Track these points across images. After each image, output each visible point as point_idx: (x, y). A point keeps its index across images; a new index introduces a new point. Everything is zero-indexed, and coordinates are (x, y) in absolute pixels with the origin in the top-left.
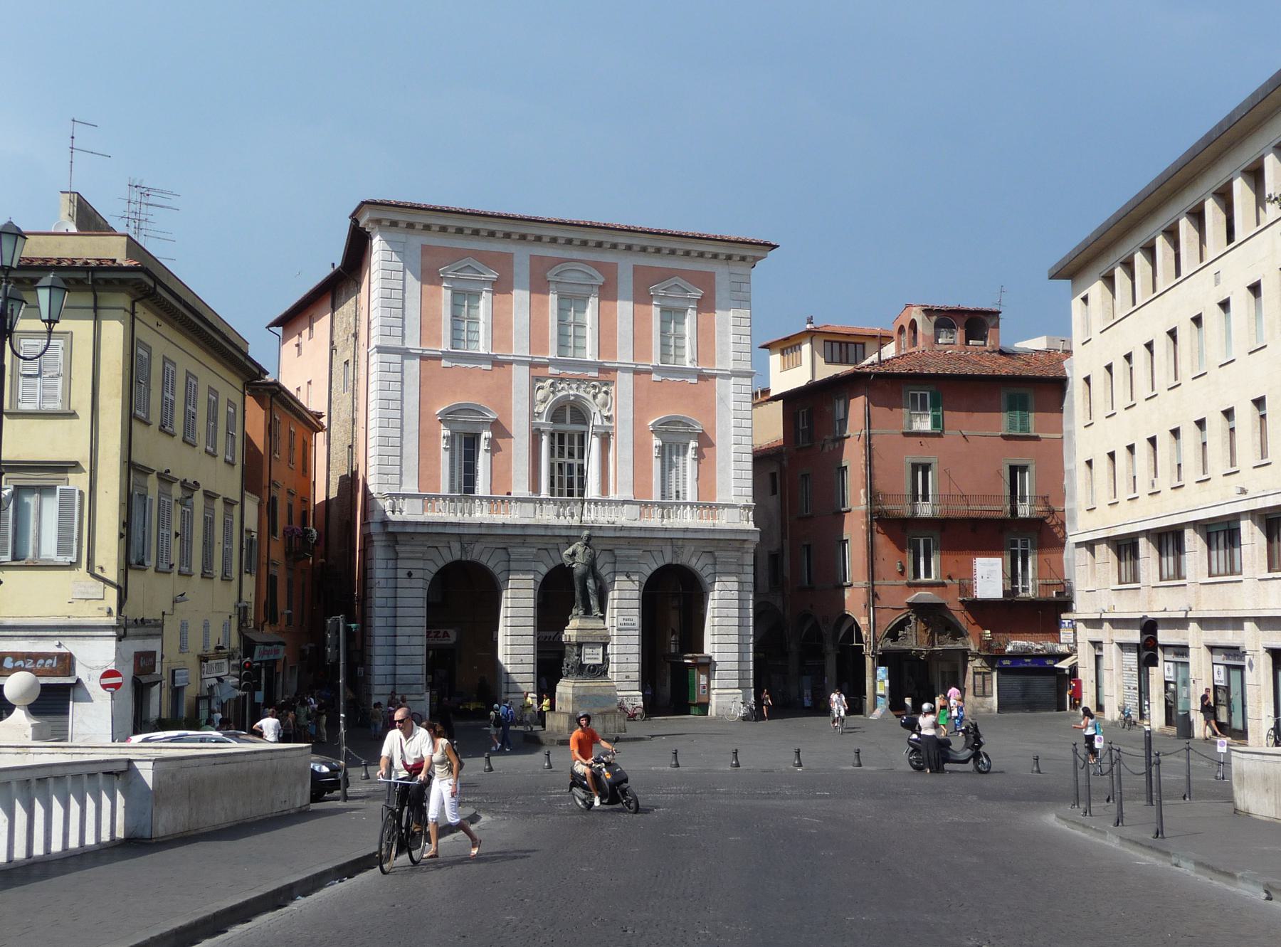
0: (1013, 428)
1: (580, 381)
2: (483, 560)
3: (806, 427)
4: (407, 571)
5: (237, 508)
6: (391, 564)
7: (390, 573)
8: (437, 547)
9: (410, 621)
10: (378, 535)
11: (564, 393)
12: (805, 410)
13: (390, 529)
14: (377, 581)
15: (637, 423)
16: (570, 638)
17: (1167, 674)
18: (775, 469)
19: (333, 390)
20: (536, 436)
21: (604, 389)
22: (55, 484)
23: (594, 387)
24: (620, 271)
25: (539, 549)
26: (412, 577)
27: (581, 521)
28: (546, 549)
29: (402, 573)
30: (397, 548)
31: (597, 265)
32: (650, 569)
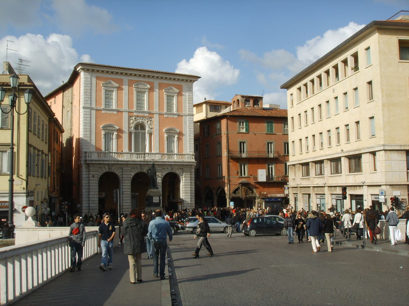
0: (268, 131)
1: (143, 117)
2: (115, 171)
4: (92, 175)
5: (47, 156)
7: (87, 176)
8: (101, 168)
11: (138, 121)
12: (207, 126)
13: (88, 162)
14: (83, 178)
15: (160, 130)
16: (149, 195)
17: (333, 203)
19: (63, 120)
20: (130, 134)
22: (6, 150)
23: (147, 119)
25: (132, 168)
26: (94, 177)
29: (91, 176)
30: (89, 168)
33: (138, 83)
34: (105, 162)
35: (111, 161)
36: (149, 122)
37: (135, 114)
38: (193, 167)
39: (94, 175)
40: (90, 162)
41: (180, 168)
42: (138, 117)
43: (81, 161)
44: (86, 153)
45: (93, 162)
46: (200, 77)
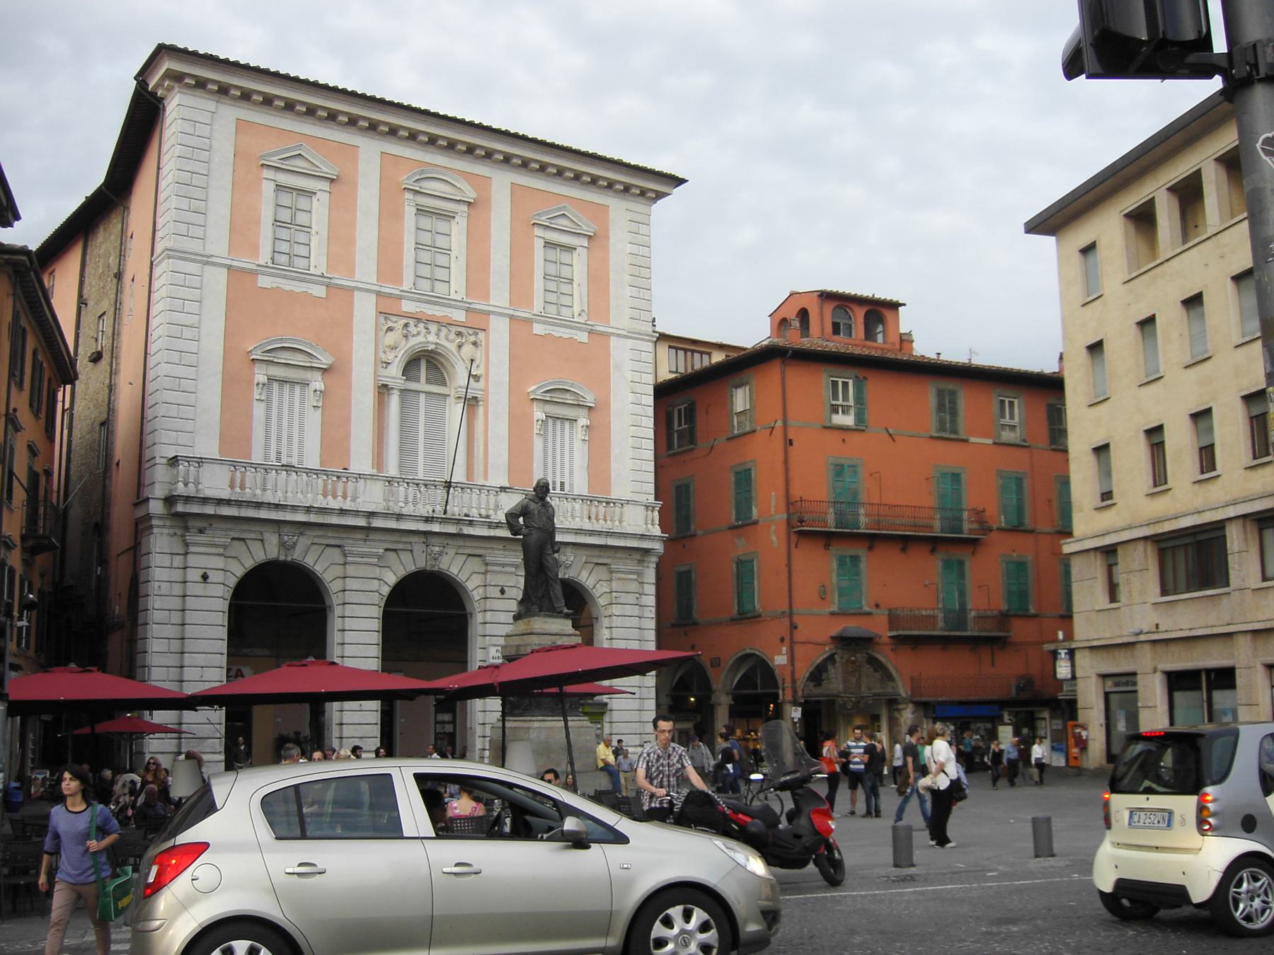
0: (942, 428)
1: (443, 324)
2: (309, 561)
3: (684, 426)
4: (201, 572)
6: (178, 561)
7: (177, 575)
8: (243, 540)
10: (161, 517)
11: (420, 339)
12: (682, 407)
13: (180, 508)
20: (383, 390)
21: (472, 339)
23: (459, 334)
24: (494, 188)
26: (208, 581)
27: (445, 512)
29: (194, 575)
31: (466, 176)
34: (264, 514)
35: (294, 508)
36: (468, 350)
37: (408, 307)
39: (209, 573)
40: (195, 509)
42: (419, 320)
43: (147, 499)
44: (174, 461)
45: (209, 510)
46: (679, 181)
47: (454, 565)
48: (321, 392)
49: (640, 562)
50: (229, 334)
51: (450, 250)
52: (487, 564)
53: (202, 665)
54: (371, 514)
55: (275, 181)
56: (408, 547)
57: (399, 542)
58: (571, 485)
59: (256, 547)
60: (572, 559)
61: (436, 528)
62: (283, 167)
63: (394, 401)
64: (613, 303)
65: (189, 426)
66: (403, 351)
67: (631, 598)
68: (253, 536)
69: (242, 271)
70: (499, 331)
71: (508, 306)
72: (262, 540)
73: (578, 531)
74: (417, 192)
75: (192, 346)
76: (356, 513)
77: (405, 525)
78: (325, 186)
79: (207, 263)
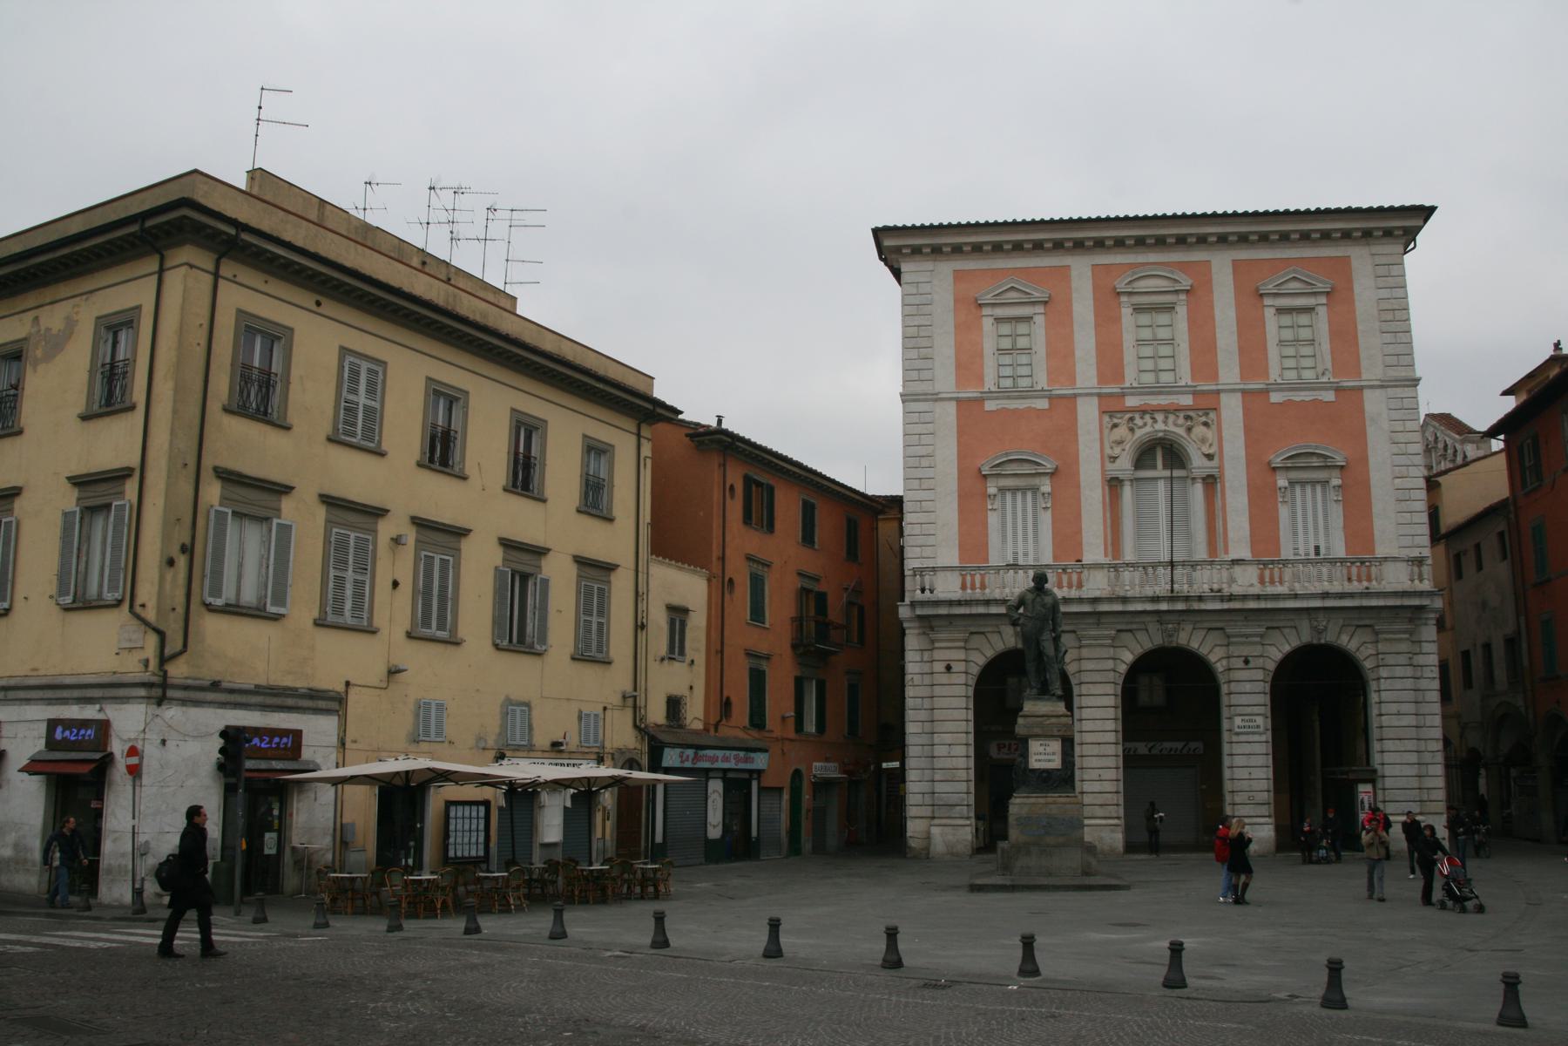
1: (1167, 411)
4: (945, 664)
7: (926, 668)
8: (983, 633)
9: (950, 726)
11: (1148, 429)
18: (1502, 527)
21: (1204, 419)
23: (1187, 418)
24: (1214, 270)
26: (952, 671)
27: (1172, 591)
28: (1130, 631)
29: (940, 667)
31: (1183, 267)
32: (1280, 651)
33: (1134, 273)
36: (1199, 430)
37: (1131, 402)
38: (1427, 619)
39: (952, 664)
41: (1358, 626)
44: (919, 571)
45: (943, 611)
46: (1426, 212)
47: (1193, 639)
48: (1049, 494)
49: (1411, 620)
50: (962, 455)
51: (1173, 339)
52: (1228, 637)
53: (949, 743)
54: (1095, 600)
55: (992, 316)
56: (1289, 624)
57: (1132, 623)
58: (1328, 548)
59: (995, 638)
60: (1324, 623)
61: (1164, 606)
62: (997, 302)
63: (1127, 492)
64: (1362, 355)
65: (931, 540)
66: (1129, 444)
67: (1402, 659)
68: (990, 629)
69: (969, 400)
70: (1232, 409)
71: (1239, 381)
72: (999, 632)
73: (1325, 595)
74: (1130, 294)
75: (929, 473)
76: (1080, 600)
77: (1131, 607)
78: (1040, 309)
79: (936, 400)
